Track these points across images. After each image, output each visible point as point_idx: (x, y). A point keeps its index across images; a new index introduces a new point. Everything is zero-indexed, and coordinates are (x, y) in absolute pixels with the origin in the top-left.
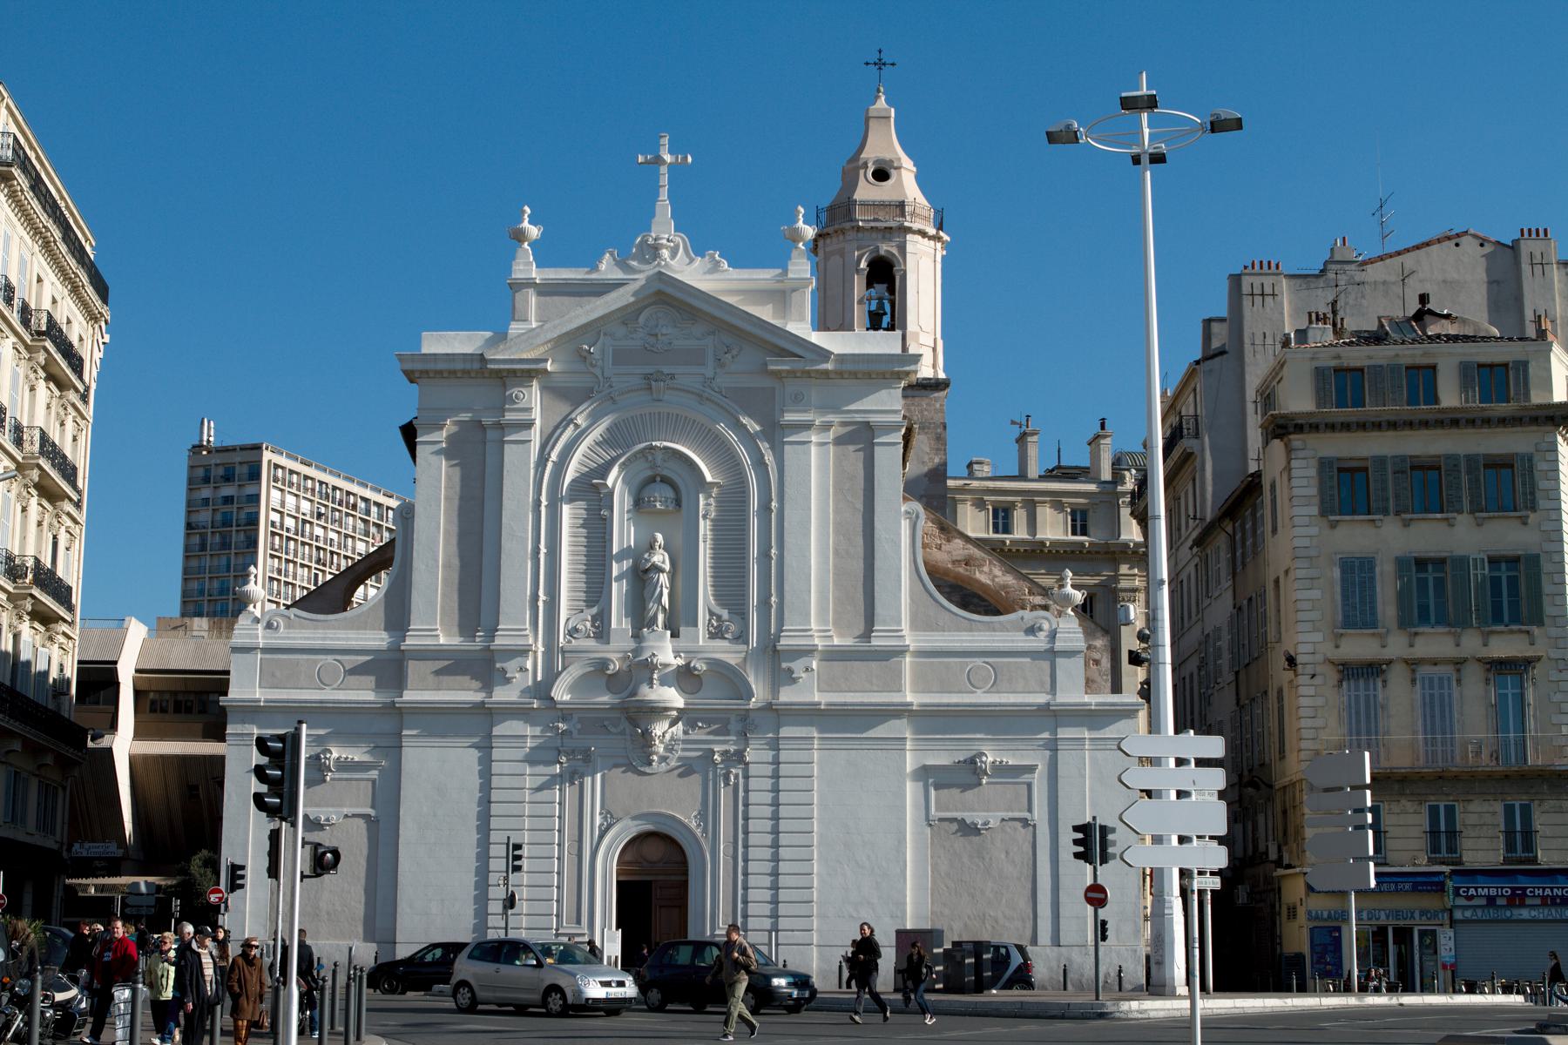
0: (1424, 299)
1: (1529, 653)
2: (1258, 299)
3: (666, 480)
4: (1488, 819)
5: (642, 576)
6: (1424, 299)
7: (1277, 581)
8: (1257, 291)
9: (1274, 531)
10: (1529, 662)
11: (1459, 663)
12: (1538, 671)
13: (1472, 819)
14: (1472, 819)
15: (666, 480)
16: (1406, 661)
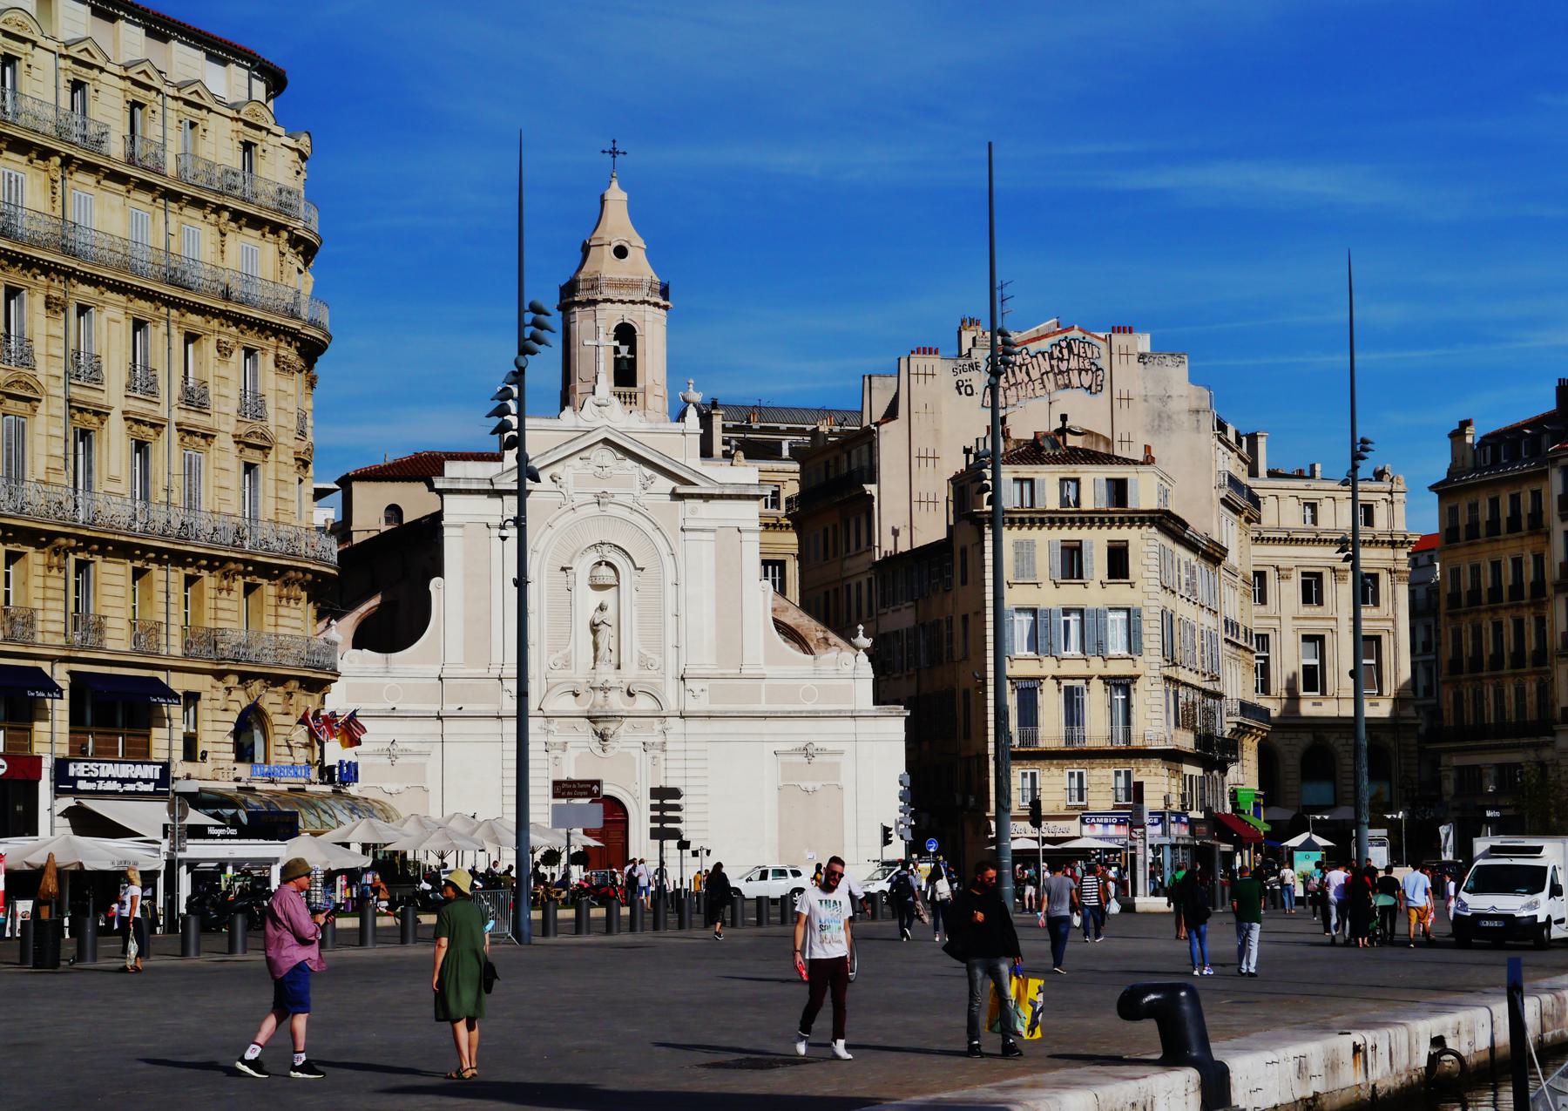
0: (1064, 418)
1: (1133, 672)
2: (921, 378)
3: (608, 564)
4: (1104, 780)
5: (594, 628)
6: (1064, 418)
7: (965, 618)
8: (922, 371)
9: (964, 582)
10: (1134, 678)
11: (1088, 679)
12: (1139, 684)
13: (1094, 780)
14: (1094, 780)
15: (608, 564)
16: (1054, 677)
